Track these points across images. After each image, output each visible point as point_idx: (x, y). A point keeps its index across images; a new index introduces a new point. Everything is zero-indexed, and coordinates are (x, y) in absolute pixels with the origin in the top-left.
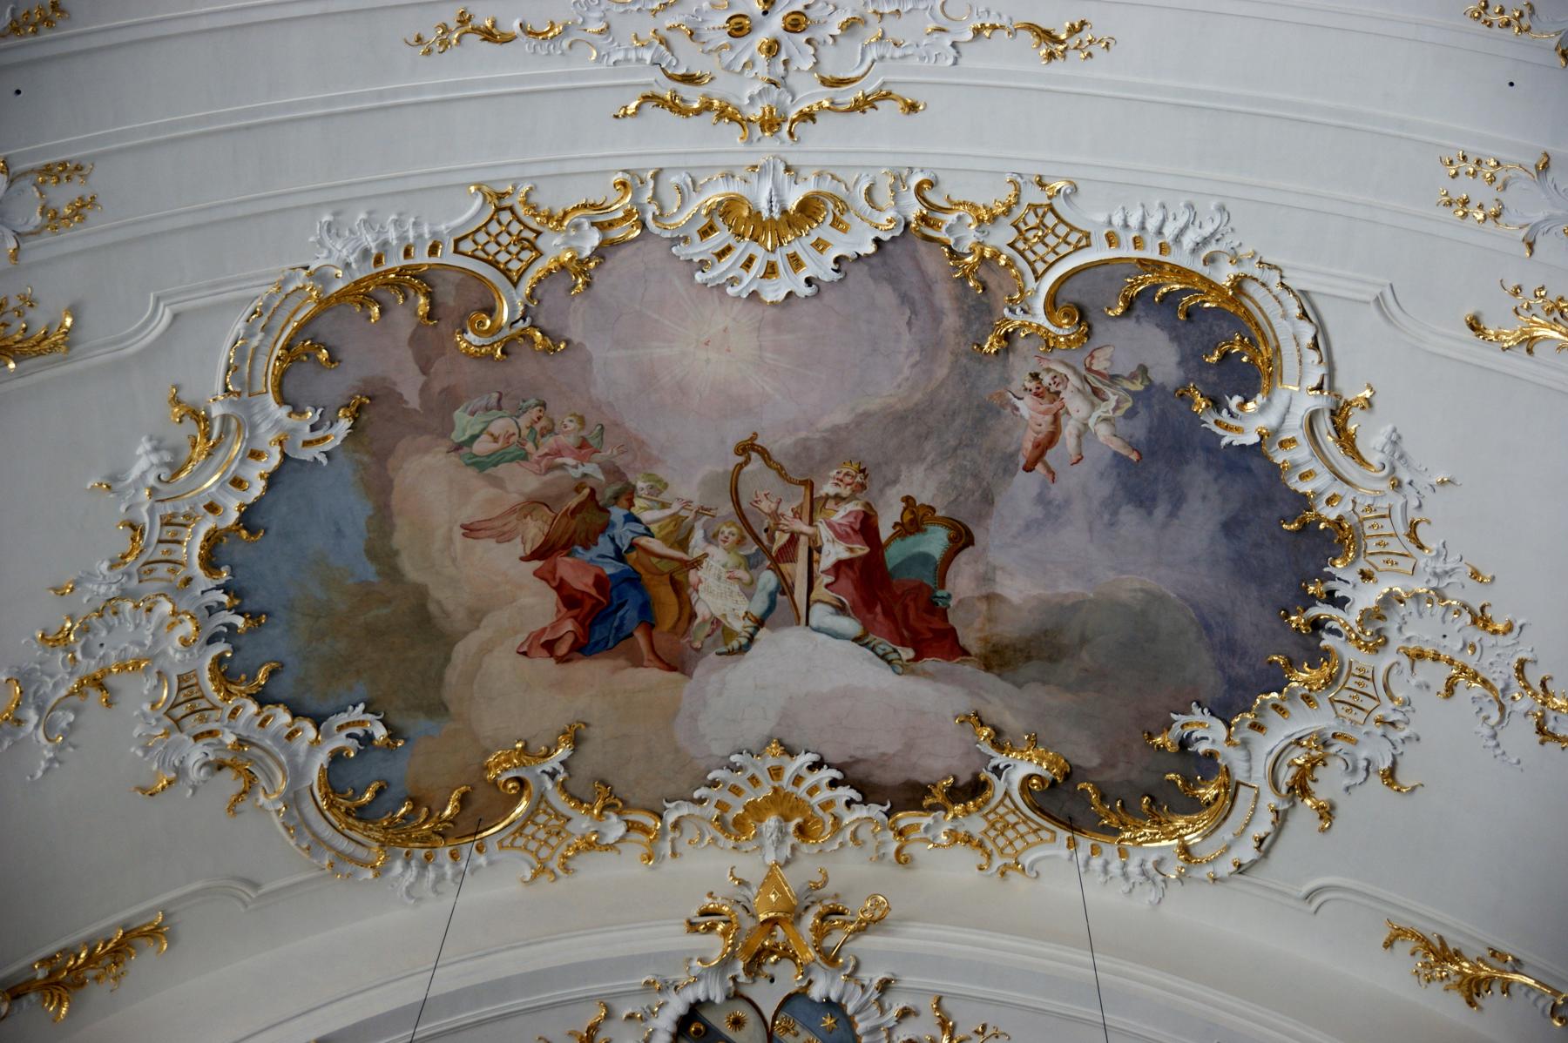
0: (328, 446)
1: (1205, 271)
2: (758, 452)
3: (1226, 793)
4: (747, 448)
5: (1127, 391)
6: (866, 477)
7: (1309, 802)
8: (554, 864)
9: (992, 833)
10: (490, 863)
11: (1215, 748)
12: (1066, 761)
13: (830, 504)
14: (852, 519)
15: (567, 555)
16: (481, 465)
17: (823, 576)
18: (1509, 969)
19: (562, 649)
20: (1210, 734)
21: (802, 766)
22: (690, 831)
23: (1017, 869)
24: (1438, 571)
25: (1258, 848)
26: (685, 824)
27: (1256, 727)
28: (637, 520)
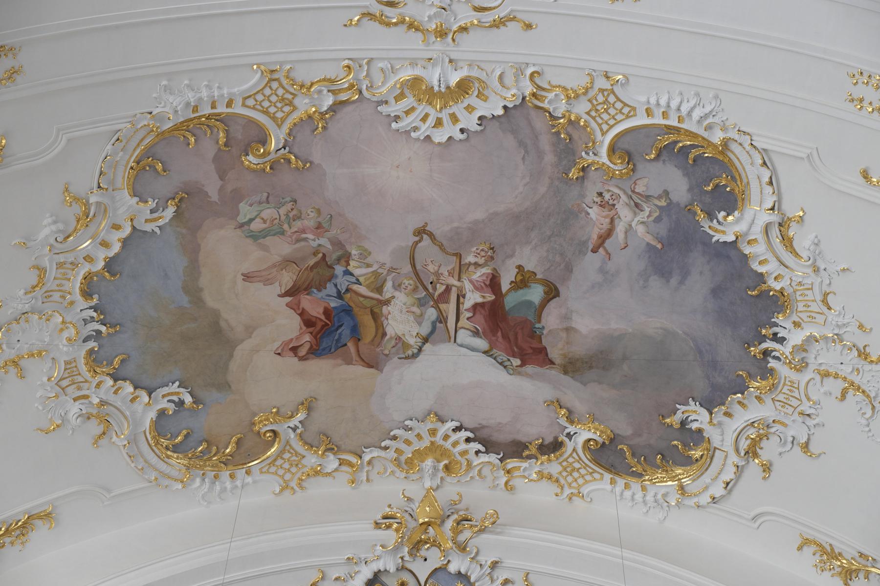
0: (161, 222)
1: (705, 135)
2: (427, 234)
3: (708, 454)
4: (421, 232)
5: (656, 205)
6: (494, 252)
7: (756, 461)
8: (293, 484)
9: (565, 474)
10: (255, 482)
12: (612, 431)
13: (472, 268)
14: (485, 278)
15: (307, 294)
16: (255, 237)
17: (466, 312)
18: (869, 565)
19: (303, 352)
20: (699, 418)
21: (449, 429)
22: (378, 467)
23: (579, 496)
24: (839, 323)
25: (726, 488)
26: (375, 462)
27: (728, 414)
28: (352, 274)
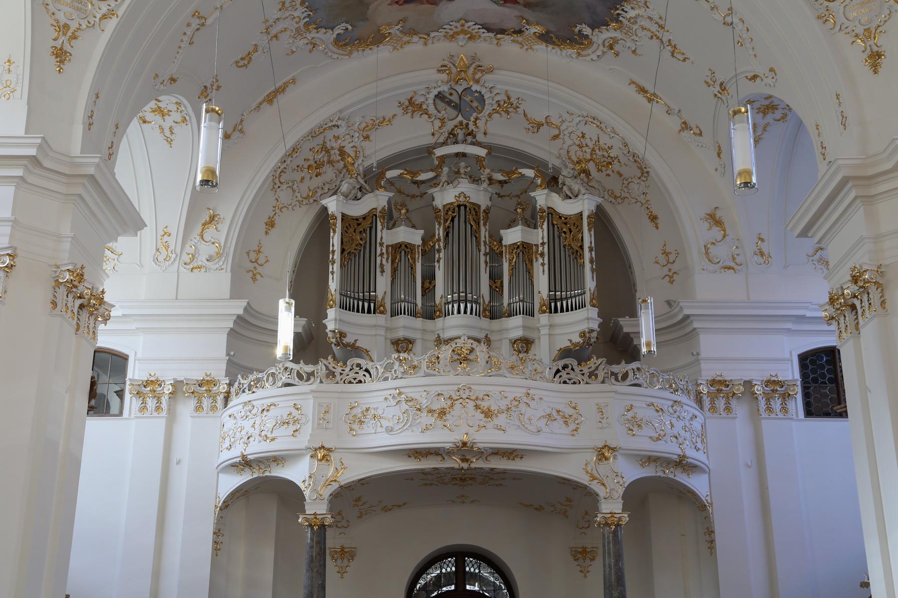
8: (398, 47)
11: (588, 34)
20: (587, 31)
22: (437, 38)
